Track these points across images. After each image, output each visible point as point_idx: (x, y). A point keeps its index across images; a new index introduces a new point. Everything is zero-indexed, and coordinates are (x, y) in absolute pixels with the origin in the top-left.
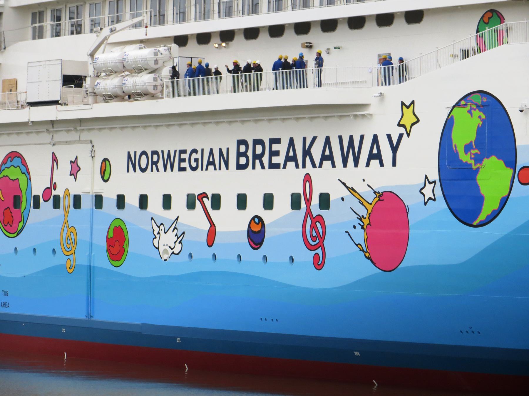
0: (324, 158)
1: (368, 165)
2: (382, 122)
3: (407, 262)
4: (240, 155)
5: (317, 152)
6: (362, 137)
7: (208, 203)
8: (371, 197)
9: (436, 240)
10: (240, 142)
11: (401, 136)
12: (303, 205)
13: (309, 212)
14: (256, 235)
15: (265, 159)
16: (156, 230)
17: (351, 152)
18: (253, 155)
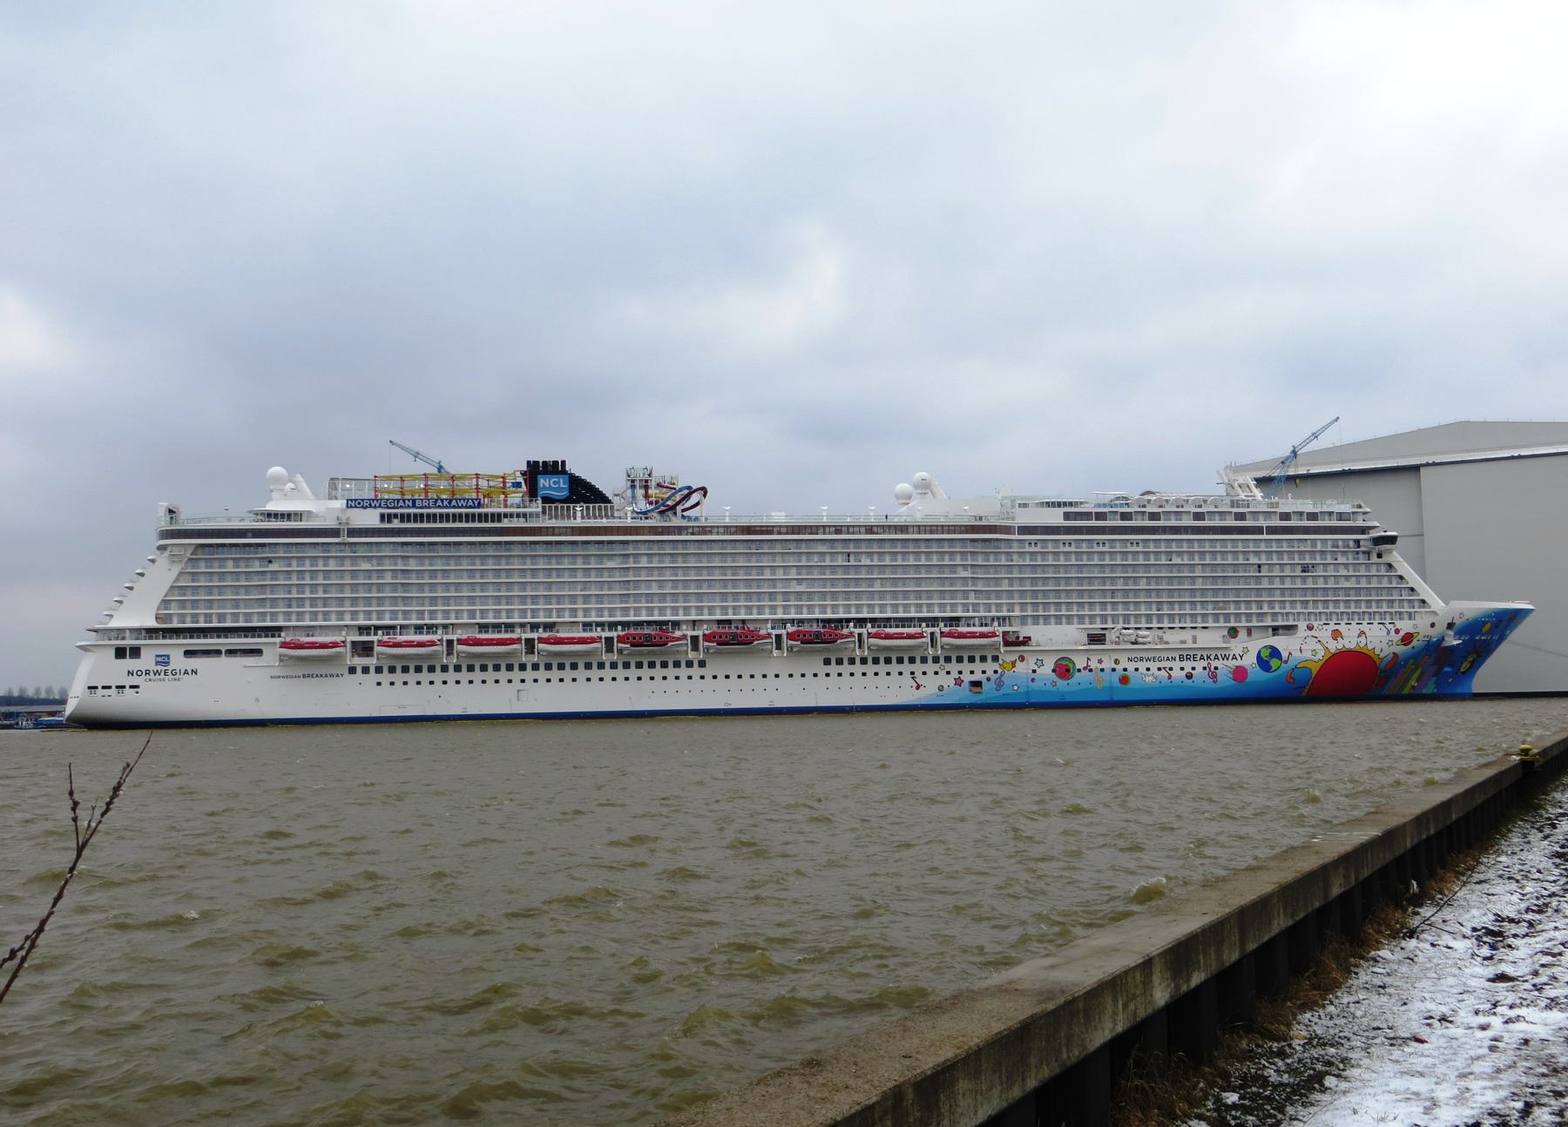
2: (1238, 651)
9: (1255, 674)
14: (1189, 676)
17: (1225, 657)
18: (1181, 658)
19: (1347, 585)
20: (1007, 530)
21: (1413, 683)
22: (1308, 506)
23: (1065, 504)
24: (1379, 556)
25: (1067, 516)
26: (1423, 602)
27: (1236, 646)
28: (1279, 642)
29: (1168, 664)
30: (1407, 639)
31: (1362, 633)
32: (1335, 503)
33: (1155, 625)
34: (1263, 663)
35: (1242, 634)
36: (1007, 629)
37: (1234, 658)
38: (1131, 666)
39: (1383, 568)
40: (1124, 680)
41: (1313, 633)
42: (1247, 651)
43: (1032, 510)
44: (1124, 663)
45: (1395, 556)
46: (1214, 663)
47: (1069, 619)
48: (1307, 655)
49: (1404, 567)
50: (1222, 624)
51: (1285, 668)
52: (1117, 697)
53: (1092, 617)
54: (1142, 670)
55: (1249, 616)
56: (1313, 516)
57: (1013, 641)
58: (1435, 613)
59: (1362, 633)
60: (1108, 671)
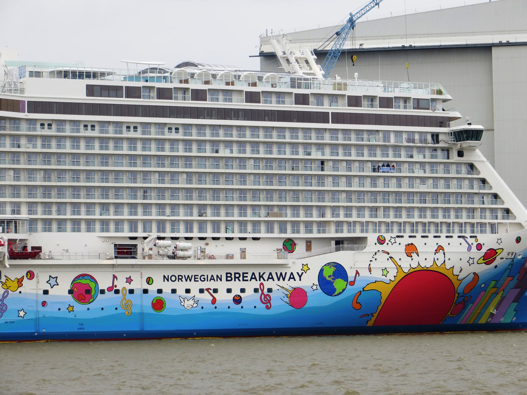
0: (269, 278)
1: (289, 280)
2: (296, 269)
3: (308, 305)
4: (227, 277)
5: (266, 277)
6: (286, 273)
7: (211, 292)
8: (291, 289)
10: (227, 274)
11: (303, 273)
12: (260, 291)
13: (263, 293)
14: (237, 300)
15: (241, 278)
16: (182, 300)
17: (281, 277)
18: (229, 277)
19: (423, 188)
20: (14, 105)
21: (492, 310)
22: (377, 89)
23: (88, 75)
24: (460, 154)
25: (91, 90)
26: (508, 211)
27: (294, 262)
28: (345, 258)
29: (212, 285)
30: (490, 256)
31: (440, 248)
32: (410, 87)
33: (196, 234)
34: (326, 285)
35: (301, 247)
36: (12, 236)
37: (292, 277)
38: (167, 287)
39: (464, 169)
40: (158, 305)
41: (384, 247)
42: (307, 268)
43: (46, 81)
44: (158, 283)
45: (477, 155)
46: (268, 284)
47: (90, 224)
48: (377, 275)
49: (486, 170)
50: (276, 235)
51: (351, 291)
52: (149, 328)
53: (118, 223)
54: (181, 292)
55: (308, 225)
56: (386, 102)
57: (22, 253)
58: (520, 225)
59: (440, 248)
60: (138, 292)
